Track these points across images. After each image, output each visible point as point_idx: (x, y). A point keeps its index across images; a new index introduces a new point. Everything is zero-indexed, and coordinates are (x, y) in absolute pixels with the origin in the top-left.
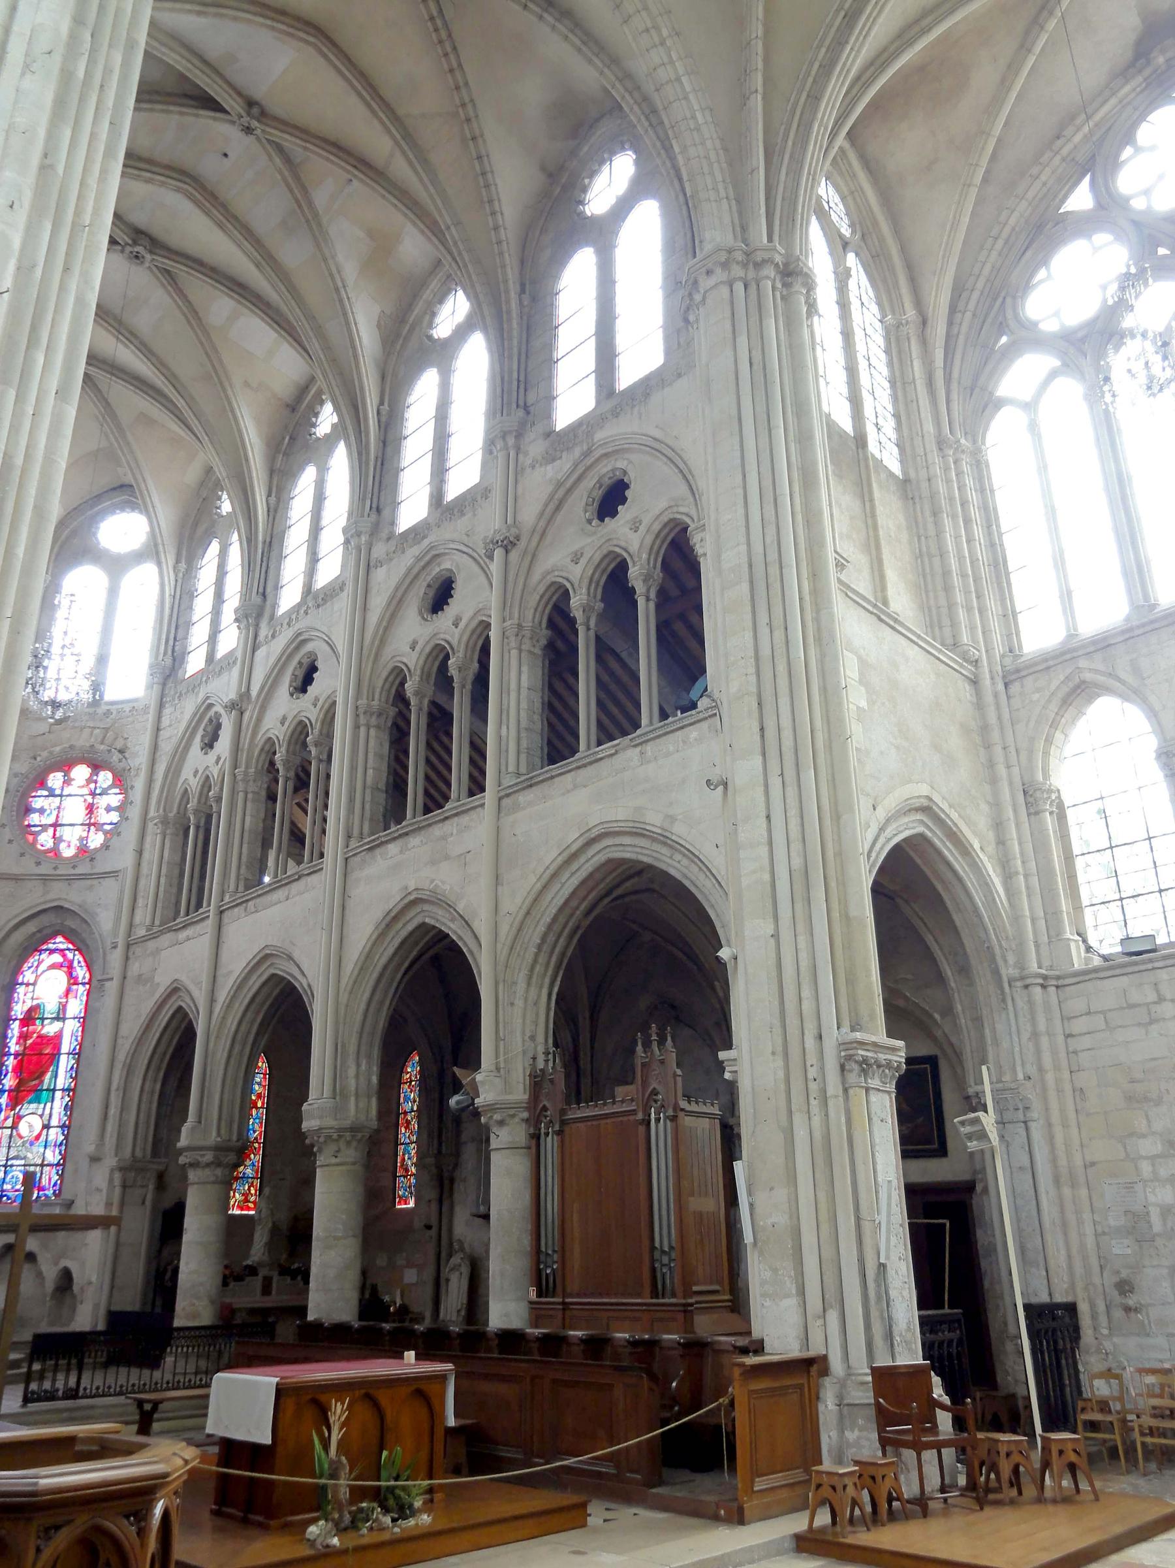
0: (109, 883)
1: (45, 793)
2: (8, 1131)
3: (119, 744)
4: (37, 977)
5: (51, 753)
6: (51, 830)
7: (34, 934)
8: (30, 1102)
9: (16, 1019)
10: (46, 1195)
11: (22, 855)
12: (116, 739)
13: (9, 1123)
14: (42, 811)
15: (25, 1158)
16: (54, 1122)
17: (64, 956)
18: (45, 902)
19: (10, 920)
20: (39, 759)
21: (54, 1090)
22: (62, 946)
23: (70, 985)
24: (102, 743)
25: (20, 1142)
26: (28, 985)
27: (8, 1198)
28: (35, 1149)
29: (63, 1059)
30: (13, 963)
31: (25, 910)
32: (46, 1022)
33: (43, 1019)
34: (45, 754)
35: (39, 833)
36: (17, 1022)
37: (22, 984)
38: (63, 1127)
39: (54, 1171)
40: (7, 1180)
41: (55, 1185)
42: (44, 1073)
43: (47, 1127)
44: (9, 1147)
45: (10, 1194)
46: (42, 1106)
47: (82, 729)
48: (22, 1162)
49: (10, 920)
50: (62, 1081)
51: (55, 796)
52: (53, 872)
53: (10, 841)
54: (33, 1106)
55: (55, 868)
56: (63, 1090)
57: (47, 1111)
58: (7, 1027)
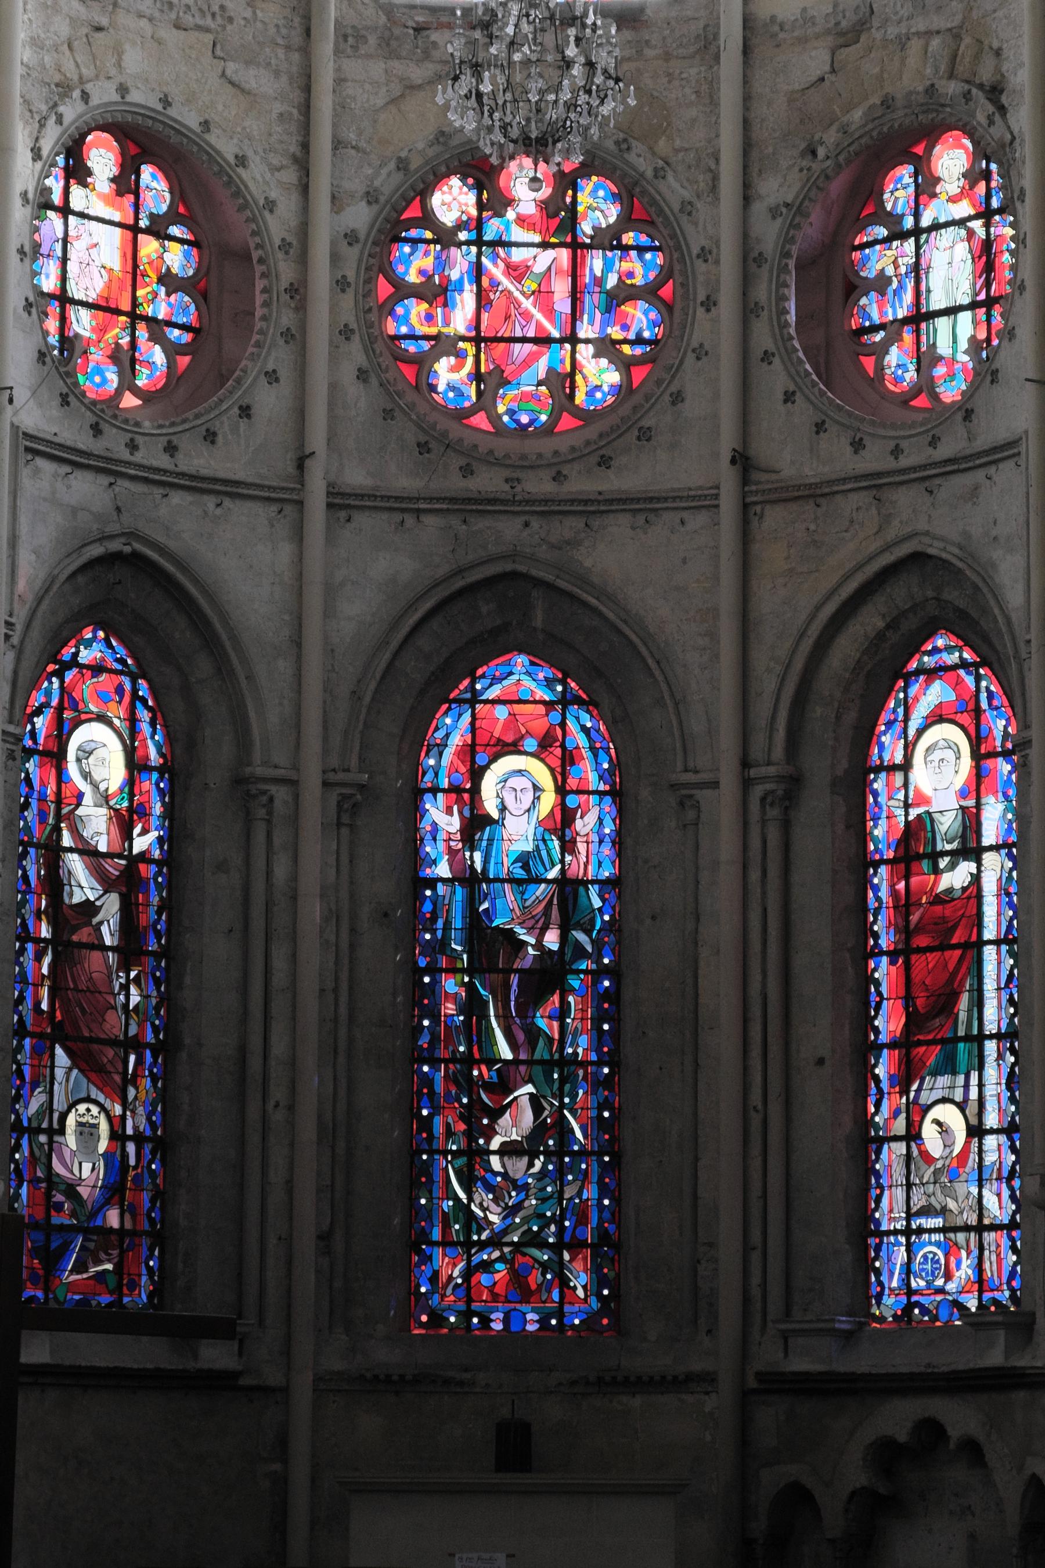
0: (1006, 473)
1: (882, 232)
2: (901, 1148)
3: (986, 74)
4: (909, 749)
5: (844, 130)
6: (908, 337)
7: (881, 636)
8: (935, 1073)
9: (883, 862)
10: (996, 1302)
11: (820, 427)
12: (977, 57)
13: (900, 1126)
14: (881, 283)
15: (944, 1211)
16: (991, 1120)
17: (957, 685)
18: (887, 548)
19: (818, 608)
20: (821, 152)
21: (981, 1038)
22: (952, 658)
23: (978, 756)
24: (951, 76)
25: (928, 1175)
26: (892, 768)
27: (924, 1311)
28: (961, 1188)
29: (990, 953)
30: (851, 717)
31: (847, 578)
32: (943, 863)
33: (935, 856)
34: (831, 137)
35: (882, 350)
36: (883, 870)
37: (878, 769)
38: (1009, 1130)
39: (1005, 1242)
40: (916, 1267)
41: (1012, 1274)
42: (955, 996)
43: (976, 1131)
44: (909, 1186)
45: (923, 1300)
46: (961, 1079)
47: (903, 42)
48: (937, 1222)
49: (818, 608)
50: (993, 1017)
51: (903, 236)
52: (890, 464)
53: (789, 397)
54: (943, 1081)
55: (896, 452)
56: (998, 1036)
57: (974, 1094)
58: (864, 883)
